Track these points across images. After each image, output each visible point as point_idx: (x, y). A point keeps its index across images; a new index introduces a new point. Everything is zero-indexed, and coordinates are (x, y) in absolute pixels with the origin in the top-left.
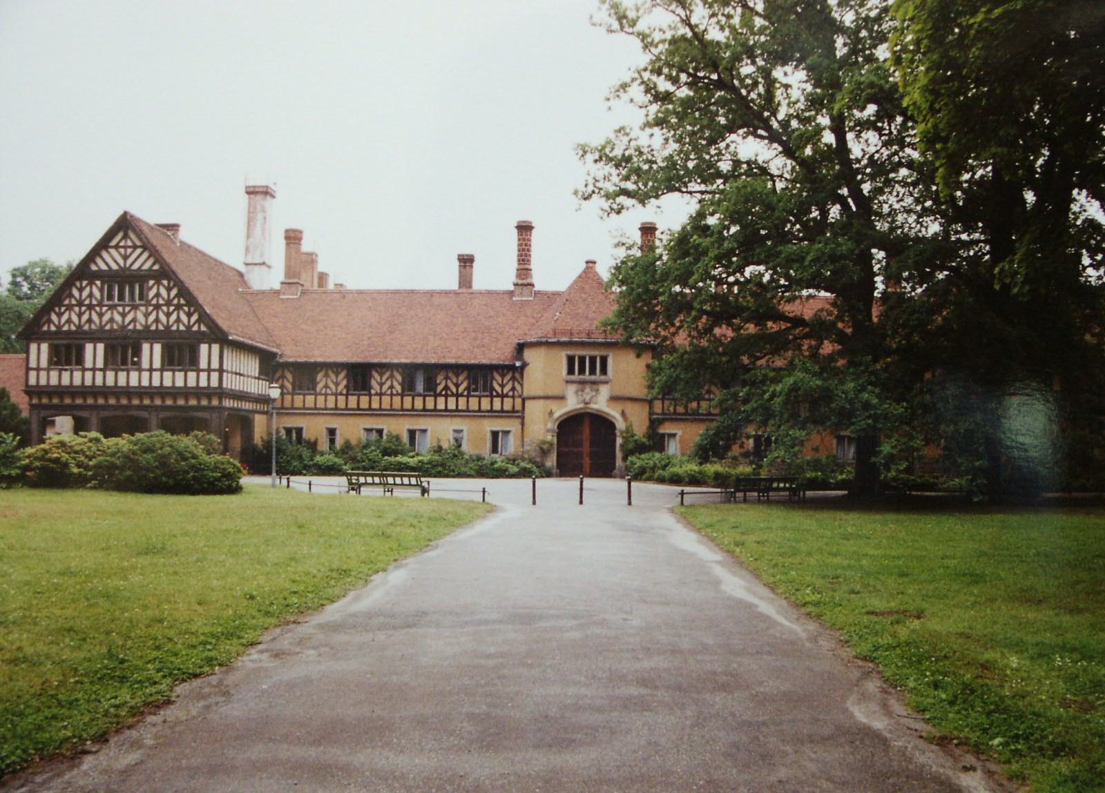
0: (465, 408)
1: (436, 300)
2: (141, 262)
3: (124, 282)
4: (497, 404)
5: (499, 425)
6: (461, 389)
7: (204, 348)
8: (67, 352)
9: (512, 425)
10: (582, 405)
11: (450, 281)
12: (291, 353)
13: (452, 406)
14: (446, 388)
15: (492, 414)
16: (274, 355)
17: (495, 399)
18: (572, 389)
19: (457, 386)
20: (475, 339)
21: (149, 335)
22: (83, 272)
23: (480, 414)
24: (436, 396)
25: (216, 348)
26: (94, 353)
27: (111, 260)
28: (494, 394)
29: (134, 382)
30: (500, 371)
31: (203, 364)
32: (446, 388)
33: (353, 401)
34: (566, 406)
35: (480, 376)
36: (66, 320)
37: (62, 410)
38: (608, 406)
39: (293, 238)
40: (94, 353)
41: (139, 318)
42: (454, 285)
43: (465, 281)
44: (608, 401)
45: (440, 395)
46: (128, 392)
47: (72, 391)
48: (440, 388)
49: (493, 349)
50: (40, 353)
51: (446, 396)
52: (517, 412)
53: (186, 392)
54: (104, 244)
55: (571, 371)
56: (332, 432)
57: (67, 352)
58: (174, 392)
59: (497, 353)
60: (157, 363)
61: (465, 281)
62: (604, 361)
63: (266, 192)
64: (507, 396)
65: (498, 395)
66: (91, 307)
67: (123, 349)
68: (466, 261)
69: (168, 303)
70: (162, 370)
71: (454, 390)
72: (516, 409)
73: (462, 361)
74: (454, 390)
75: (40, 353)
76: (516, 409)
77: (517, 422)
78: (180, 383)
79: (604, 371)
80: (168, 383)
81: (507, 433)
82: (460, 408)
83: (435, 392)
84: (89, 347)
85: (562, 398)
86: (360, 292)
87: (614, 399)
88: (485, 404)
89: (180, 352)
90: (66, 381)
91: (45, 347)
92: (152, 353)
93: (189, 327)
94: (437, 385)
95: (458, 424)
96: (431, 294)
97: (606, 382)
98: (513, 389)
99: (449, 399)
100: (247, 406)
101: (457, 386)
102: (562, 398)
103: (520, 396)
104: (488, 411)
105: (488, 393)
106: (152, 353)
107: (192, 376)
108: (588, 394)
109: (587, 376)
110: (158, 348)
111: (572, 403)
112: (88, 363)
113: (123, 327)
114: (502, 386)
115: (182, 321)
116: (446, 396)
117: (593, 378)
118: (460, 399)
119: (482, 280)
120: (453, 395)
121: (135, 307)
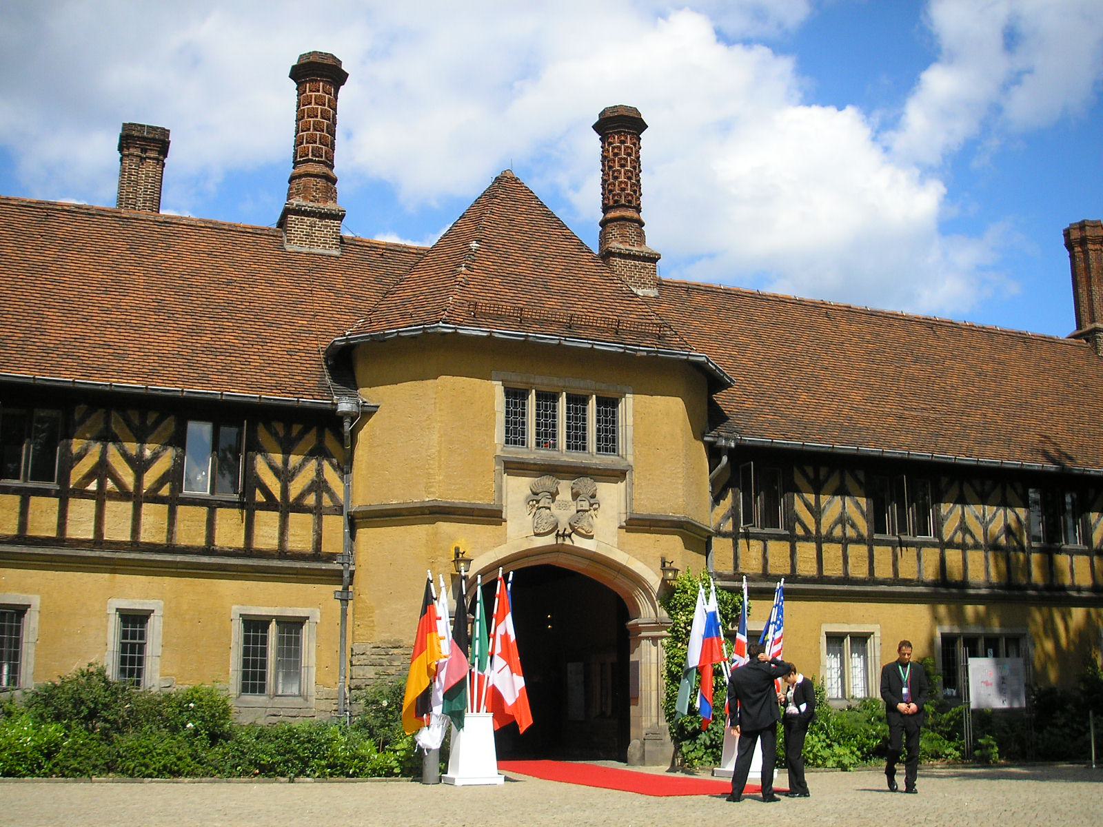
0: (161, 539)
5: (272, 598)
6: (149, 479)
10: (550, 540)
14: (102, 470)
15: (250, 564)
17: (260, 515)
18: (518, 488)
19: (139, 466)
20: (195, 331)
23: (207, 563)
24: (64, 496)
28: (259, 497)
30: (279, 428)
32: (102, 470)
34: (503, 540)
38: (621, 546)
44: (621, 527)
45: (82, 494)
48: (78, 472)
49: (257, 361)
51: (100, 497)
52: (331, 557)
55: (515, 433)
62: (609, 405)
64: (298, 507)
65: (270, 504)
71: (128, 478)
72: (326, 548)
73: (161, 386)
74: (128, 478)
76: (326, 548)
77: (328, 591)
79: (608, 441)
81: (292, 626)
82: (144, 537)
83: (64, 478)
85: (492, 516)
87: (637, 524)
88: (229, 530)
94: (72, 460)
95: (135, 591)
97: (617, 475)
98: (319, 485)
99: (110, 505)
101: (139, 466)
102: (492, 516)
103: (338, 510)
104: (235, 553)
105: (236, 497)
108: (565, 506)
109: (562, 454)
111: (520, 534)
114: (286, 476)
116: (100, 497)
117: (575, 458)
118: (146, 508)
120: (123, 495)
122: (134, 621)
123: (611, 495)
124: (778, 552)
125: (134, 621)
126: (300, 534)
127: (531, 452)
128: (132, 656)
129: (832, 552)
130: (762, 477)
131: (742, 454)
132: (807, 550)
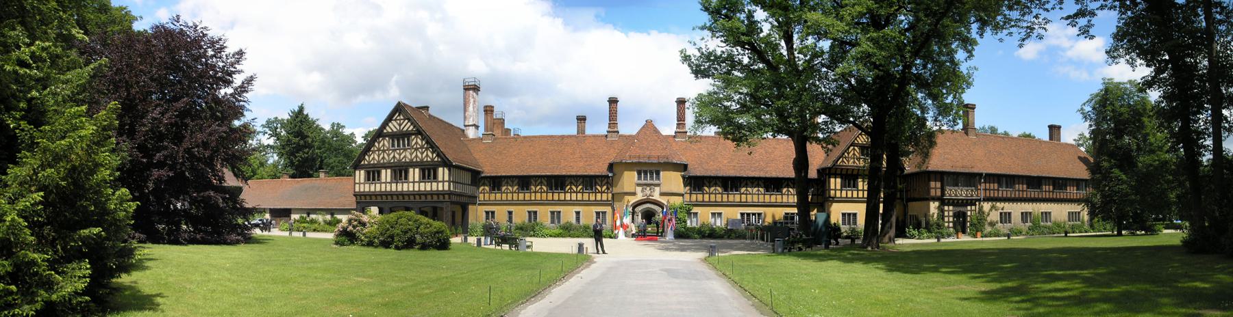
1: (566, 141)
2: (407, 126)
3: (400, 137)
4: (599, 197)
7: (441, 169)
8: (373, 174)
9: (608, 209)
11: (572, 130)
12: (488, 170)
13: (574, 197)
15: (596, 203)
16: (479, 173)
18: (639, 189)
21: (413, 164)
22: (379, 134)
25: (446, 171)
26: (386, 175)
27: (393, 127)
29: (405, 189)
31: (440, 178)
33: (521, 196)
35: (589, 182)
36: (373, 158)
37: (374, 204)
39: (489, 110)
40: (386, 175)
41: (407, 156)
42: (575, 133)
43: (581, 130)
46: (403, 194)
47: (375, 195)
50: (360, 175)
53: (432, 193)
54: (390, 119)
55: (639, 178)
56: (510, 213)
57: (373, 174)
58: (426, 194)
59: (600, 169)
60: (417, 179)
61: (581, 130)
63: (476, 89)
66: (384, 151)
67: (400, 171)
68: (582, 119)
69: (422, 147)
70: (419, 182)
75: (360, 175)
78: (428, 189)
80: (422, 189)
81: (604, 213)
84: (383, 171)
85: (634, 194)
86: (525, 137)
87: (662, 194)
89: (428, 172)
90: (372, 189)
91: (362, 172)
92: (414, 174)
93: (433, 159)
96: (563, 137)
97: (658, 185)
100: (463, 200)
106: (414, 174)
107: (434, 184)
109: (649, 181)
110: (417, 170)
112: (383, 180)
113: (400, 160)
115: (429, 156)
119: (590, 130)
121: (405, 150)
122: (578, 213)
123: (657, 189)
124: (700, 197)
125: (578, 213)
126: (605, 197)
127: (643, 181)
128: (578, 219)
129: (713, 197)
130: (696, 183)
131: (690, 178)
132: (706, 197)
